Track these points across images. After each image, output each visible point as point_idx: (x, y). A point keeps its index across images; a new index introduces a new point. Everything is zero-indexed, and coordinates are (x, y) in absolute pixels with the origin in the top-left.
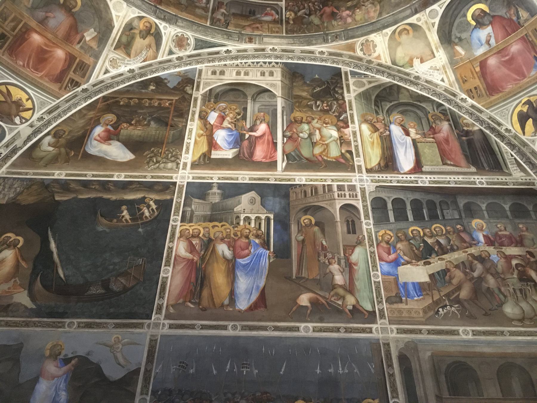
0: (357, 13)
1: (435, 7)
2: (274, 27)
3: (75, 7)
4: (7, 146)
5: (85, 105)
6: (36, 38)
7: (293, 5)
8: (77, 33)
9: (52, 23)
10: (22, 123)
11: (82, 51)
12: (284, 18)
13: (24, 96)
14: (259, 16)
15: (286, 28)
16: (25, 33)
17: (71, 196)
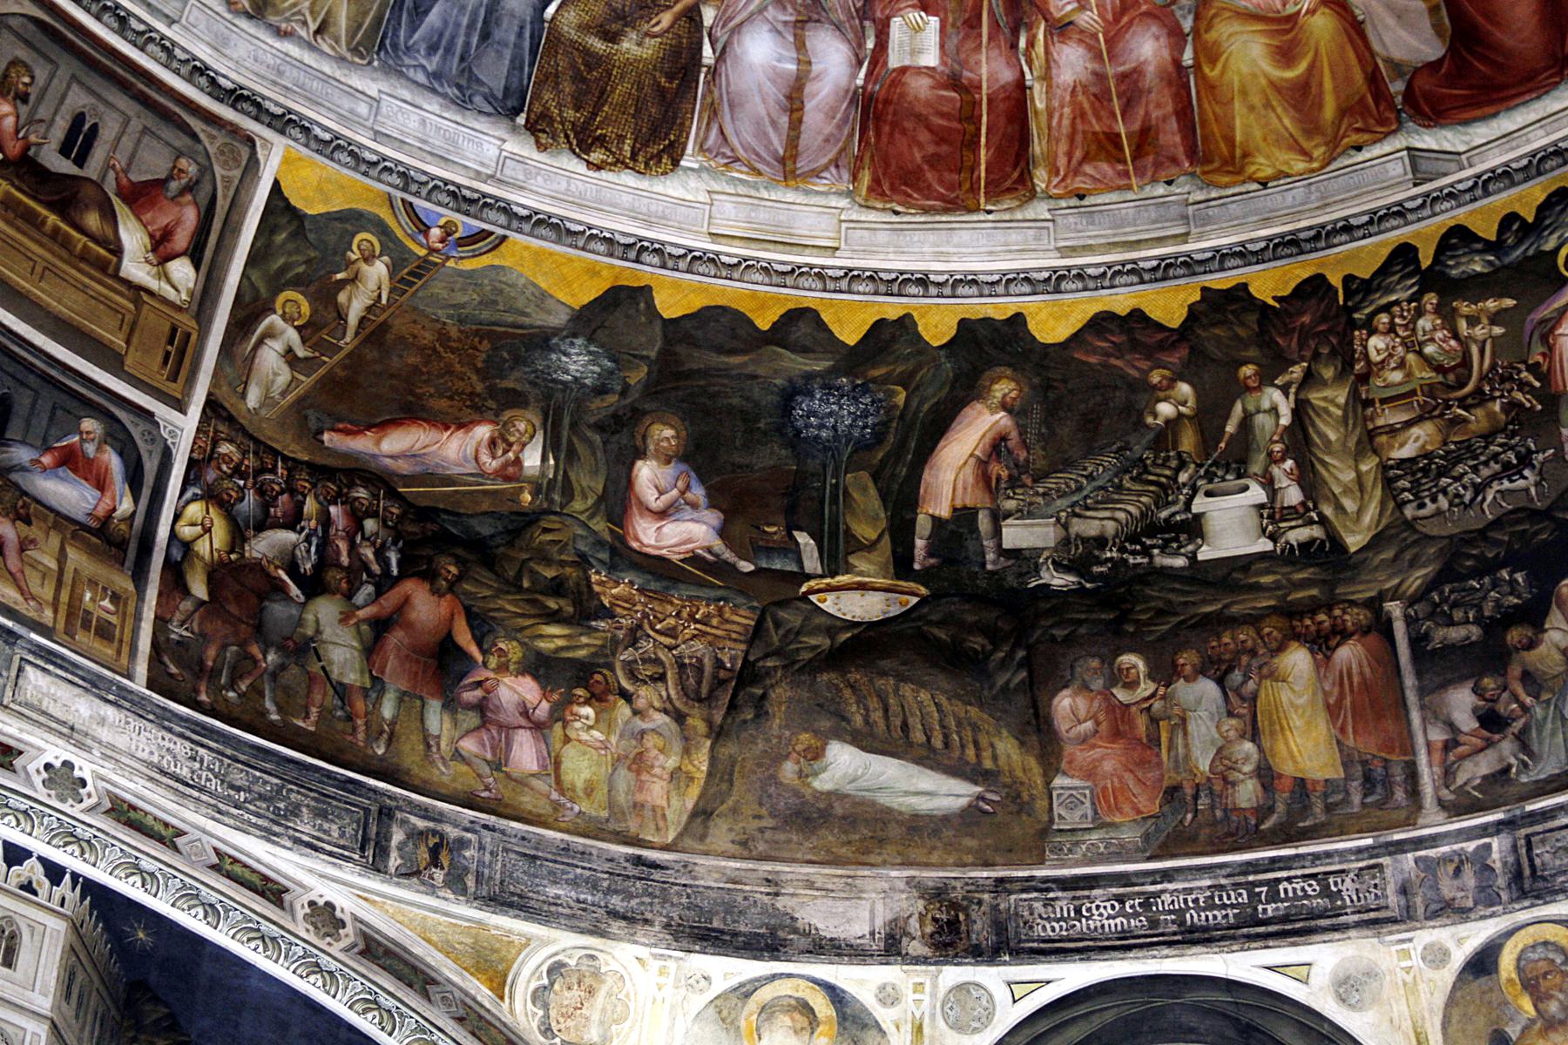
0: (577, 729)
1: (993, 977)
2: (93, 583)
7: (237, 471)
12: (163, 532)
14: (22, 454)
15: (161, 622)
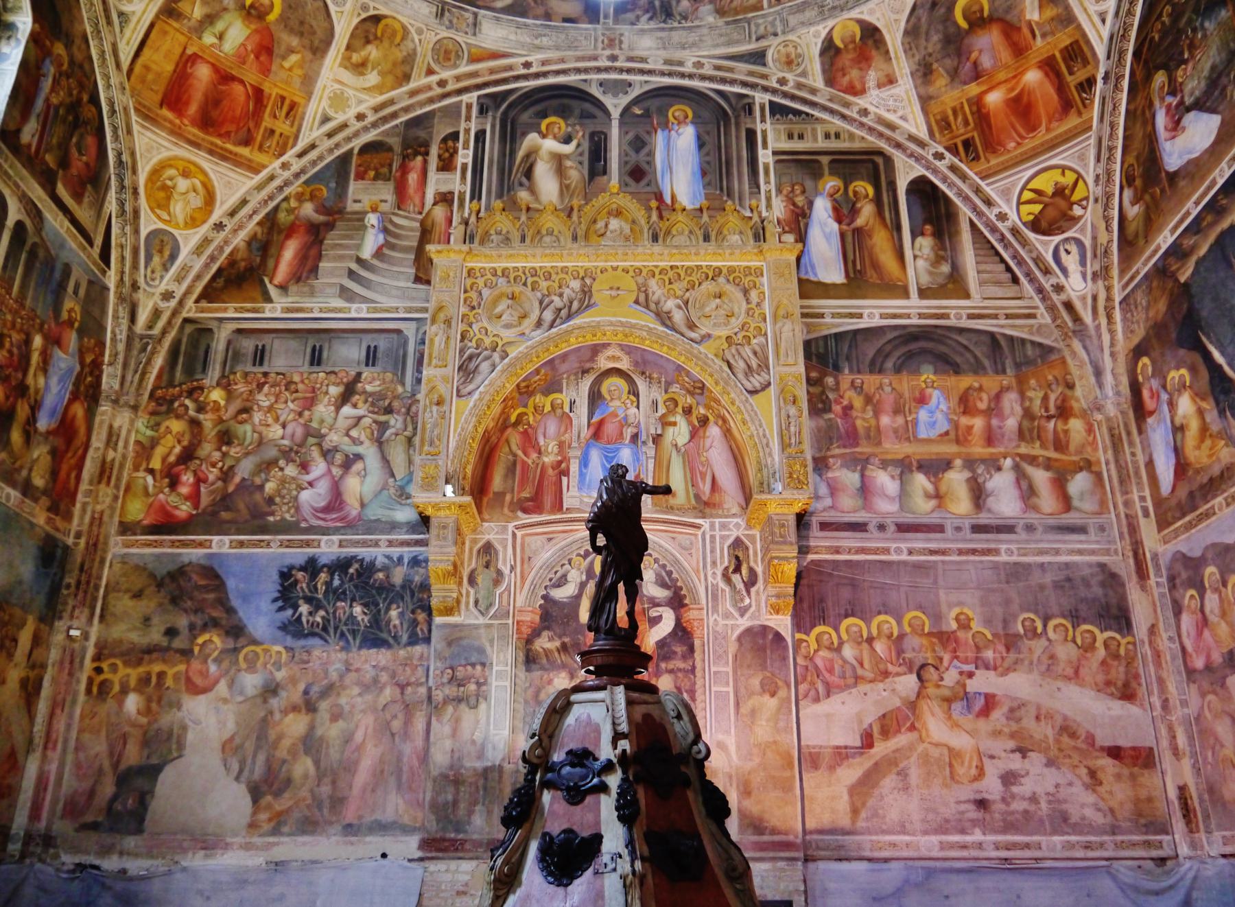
3: (982, 10)
4: (1095, 256)
5: (1124, 96)
6: (994, 99)
8: (1019, 29)
9: (986, 62)
10: (1085, 208)
11: (1049, 39)
13: (1055, 176)
16: (979, 110)
17: (1194, 259)
